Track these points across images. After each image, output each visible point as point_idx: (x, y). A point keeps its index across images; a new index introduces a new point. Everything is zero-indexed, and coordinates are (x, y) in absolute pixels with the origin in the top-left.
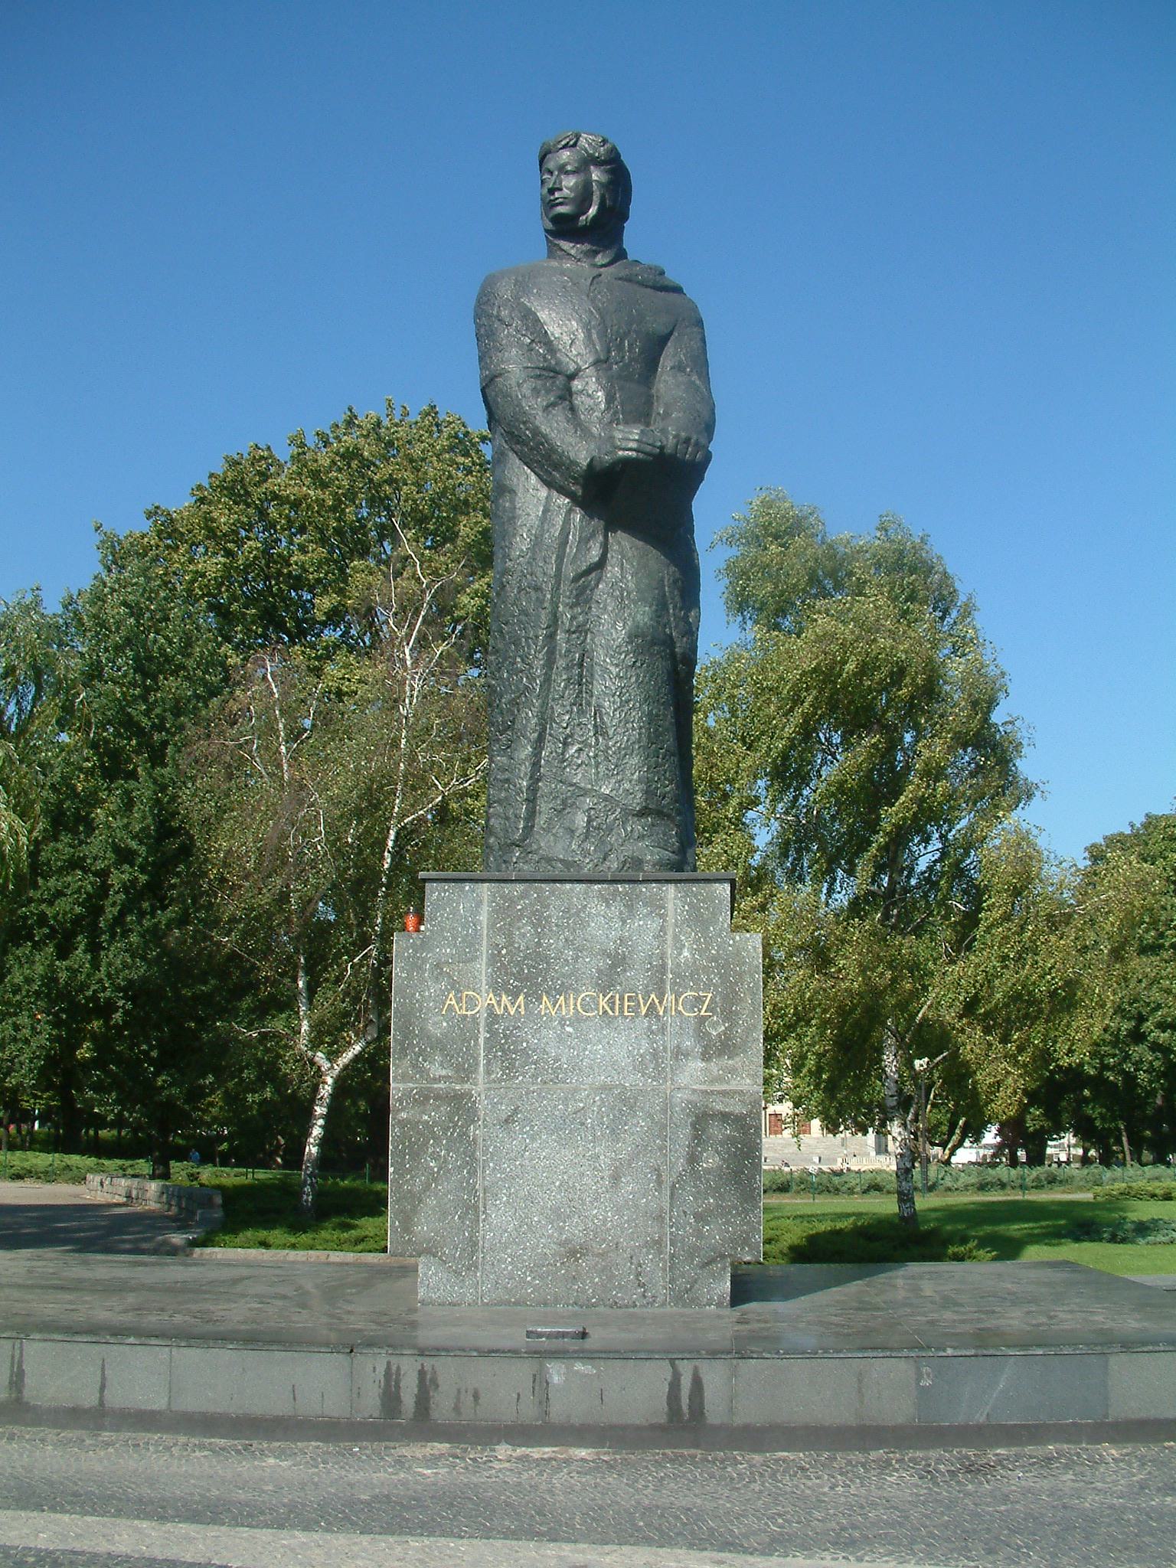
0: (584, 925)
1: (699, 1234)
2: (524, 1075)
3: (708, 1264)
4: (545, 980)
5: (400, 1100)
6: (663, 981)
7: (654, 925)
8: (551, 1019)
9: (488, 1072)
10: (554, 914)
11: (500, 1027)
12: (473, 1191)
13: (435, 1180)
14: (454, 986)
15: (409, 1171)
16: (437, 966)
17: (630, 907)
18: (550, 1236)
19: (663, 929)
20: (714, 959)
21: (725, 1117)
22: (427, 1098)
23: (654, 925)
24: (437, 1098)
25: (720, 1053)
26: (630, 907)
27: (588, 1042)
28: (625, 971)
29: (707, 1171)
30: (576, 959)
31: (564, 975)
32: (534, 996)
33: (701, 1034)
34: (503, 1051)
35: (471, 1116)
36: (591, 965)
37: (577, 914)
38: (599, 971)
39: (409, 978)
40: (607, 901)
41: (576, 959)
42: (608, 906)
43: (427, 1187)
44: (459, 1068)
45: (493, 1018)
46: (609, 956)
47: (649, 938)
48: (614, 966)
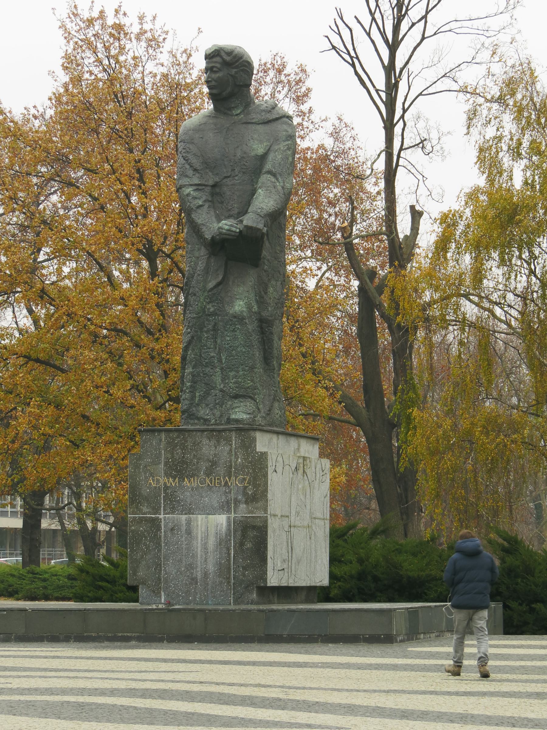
0: (201, 449)
1: (244, 575)
2: (178, 510)
3: (247, 587)
4: (186, 472)
5: (132, 522)
6: (231, 472)
7: (227, 448)
8: (188, 488)
9: (164, 510)
10: (189, 444)
11: (169, 491)
12: (159, 559)
13: (145, 554)
14: (152, 475)
15: (135, 550)
16: (145, 466)
17: (218, 442)
18: (188, 576)
19: (231, 450)
20: (250, 462)
21: (254, 527)
22: (142, 521)
23: (227, 448)
24: (146, 520)
25: (252, 501)
26: (218, 442)
27: (202, 497)
28: (216, 468)
29: (247, 549)
30: (198, 463)
31: (193, 470)
32: (182, 479)
33: (245, 494)
34: (170, 501)
35: (159, 528)
36: (204, 465)
37: (199, 443)
38: (206, 468)
39: (135, 472)
40: (209, 439)
41: (198, 463)
42: (210, 441)
43: (142, 557)
44: (154, 508)
45: (166, 488)
46: (210, 461)
47: (225, 454)
48: (212, 466)
